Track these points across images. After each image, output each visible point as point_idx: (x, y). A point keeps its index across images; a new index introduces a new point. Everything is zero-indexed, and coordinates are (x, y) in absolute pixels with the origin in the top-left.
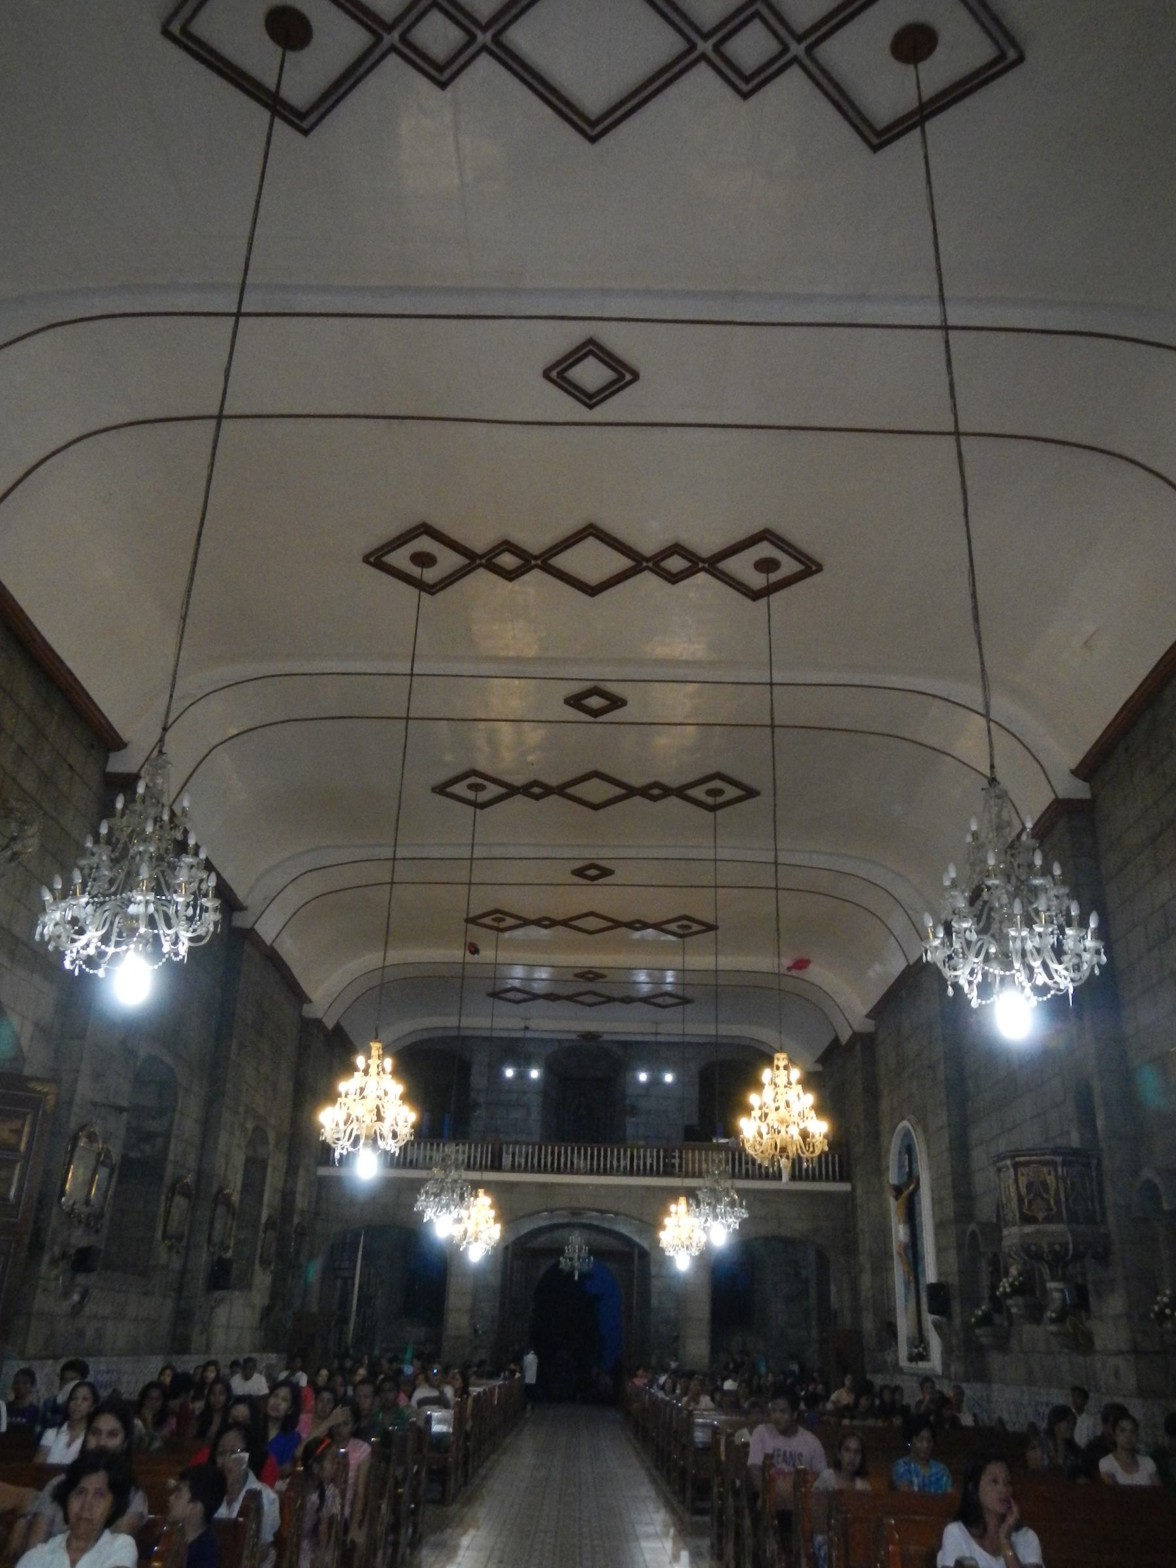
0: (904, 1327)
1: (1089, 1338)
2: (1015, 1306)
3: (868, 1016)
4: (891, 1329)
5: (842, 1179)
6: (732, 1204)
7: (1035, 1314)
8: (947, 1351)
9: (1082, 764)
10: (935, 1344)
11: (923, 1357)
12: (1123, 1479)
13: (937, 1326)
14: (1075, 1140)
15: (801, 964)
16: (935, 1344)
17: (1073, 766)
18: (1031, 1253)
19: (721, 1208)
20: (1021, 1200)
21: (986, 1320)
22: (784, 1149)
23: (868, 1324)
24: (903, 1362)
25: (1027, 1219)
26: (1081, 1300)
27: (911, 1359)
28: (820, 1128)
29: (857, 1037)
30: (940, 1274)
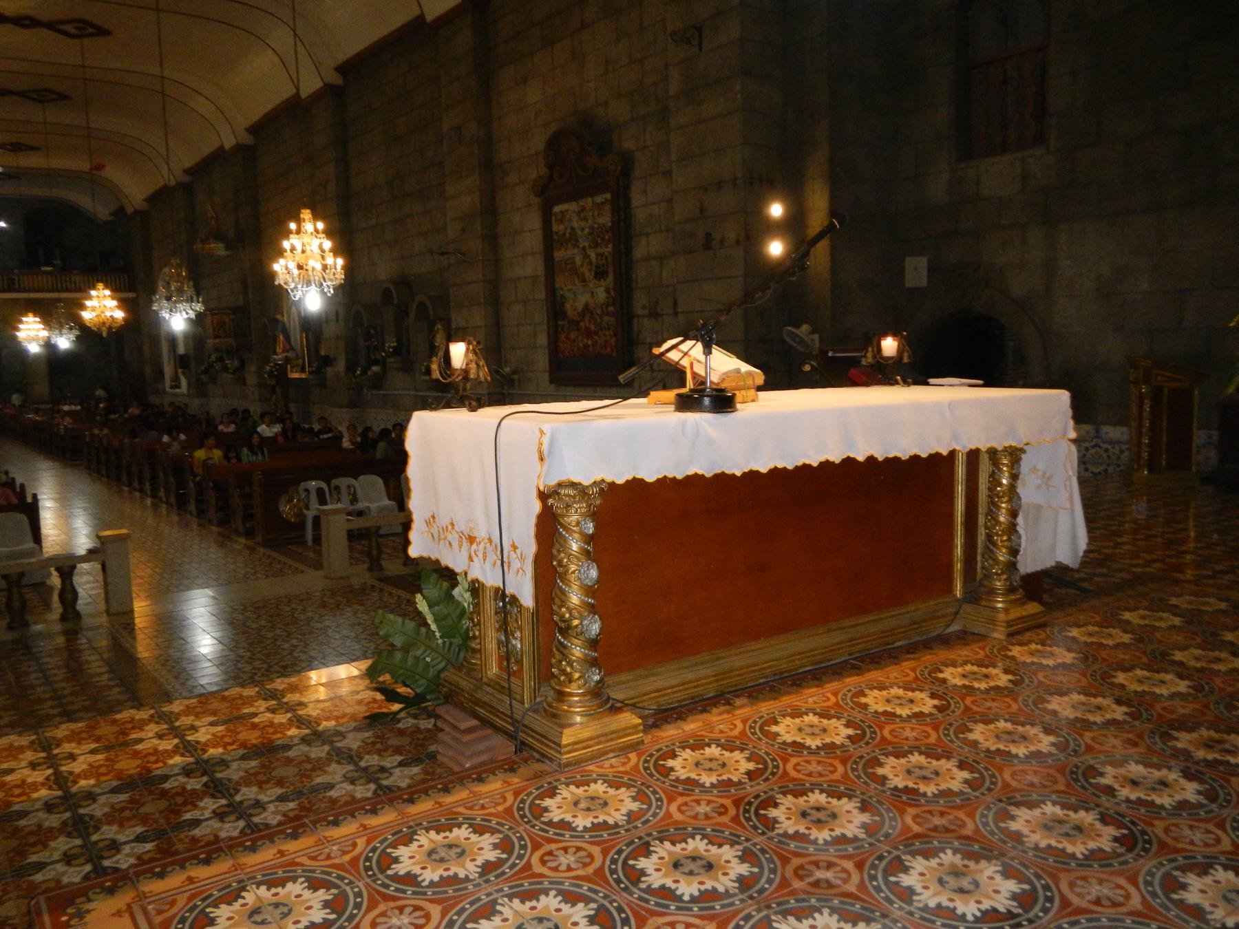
0: (168, 371)
1: (244, 380)
2: (218, 366)
3: (145, 200)
4: (161, 372)
5: (130, 291)
6: (71, 328)
7: (225, 369)
8: (189, 385)
9: (252, 126)
10: (184, 382)
11: (178, 386)
12: (226, 430)
13: (184, 373)
14: (241, 302)
15: (100, 167)
16: (184, 382)
17: (247, 126)
18: (217, 350)
19: (64, 331)
20: (214, 328)
21: (206, 372)
22: (104, 323)
23: (148, 371)
24: (168, 389)
25: (217, 337)
26: (242, 364)
27: (172, 387)
28: (120, 315)
29: (137, 212)
30: (186, 349)
